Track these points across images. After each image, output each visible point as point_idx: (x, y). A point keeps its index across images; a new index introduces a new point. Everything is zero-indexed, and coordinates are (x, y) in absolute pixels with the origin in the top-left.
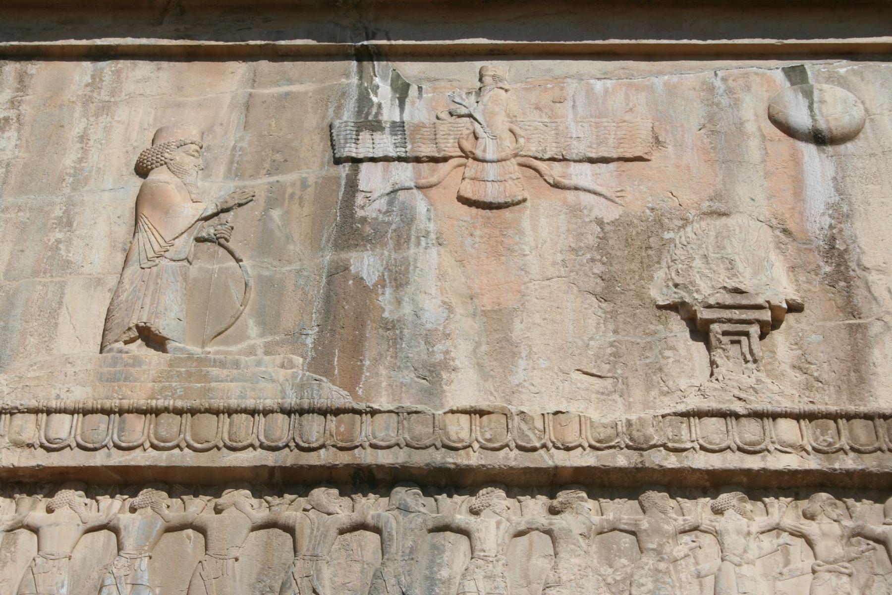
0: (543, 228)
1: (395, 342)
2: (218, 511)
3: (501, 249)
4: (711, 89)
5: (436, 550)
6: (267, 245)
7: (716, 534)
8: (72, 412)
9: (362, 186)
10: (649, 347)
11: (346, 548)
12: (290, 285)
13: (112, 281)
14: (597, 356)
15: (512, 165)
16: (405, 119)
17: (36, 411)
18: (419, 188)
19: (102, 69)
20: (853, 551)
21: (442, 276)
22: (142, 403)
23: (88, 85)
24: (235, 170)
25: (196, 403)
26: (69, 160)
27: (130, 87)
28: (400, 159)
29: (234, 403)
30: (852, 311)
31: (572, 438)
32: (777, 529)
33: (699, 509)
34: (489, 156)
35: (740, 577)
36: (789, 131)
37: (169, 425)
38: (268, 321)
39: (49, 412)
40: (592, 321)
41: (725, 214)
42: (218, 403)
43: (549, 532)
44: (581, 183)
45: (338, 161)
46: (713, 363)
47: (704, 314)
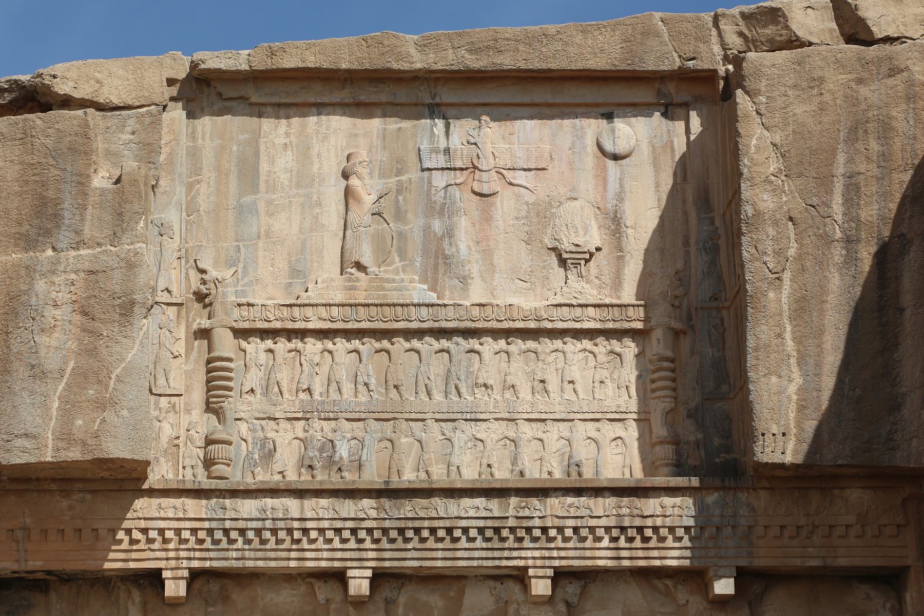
0: (506, 206)
2: (393, 344)
3: (487, 217)
7: (564, 353)
8: (338, 305)
10: (544, 268)
15: (493, 173)
16: (450, 146)
18: (456, 185)
21: (466, 233)
22: (363, 301)
24: (382, 175)
25: (382, 301)
28: (448, 169)
29: (395, 301)
31: (515, 316)
33: (558, 344)
34: (484, 168)
35: (570, 370)
38: (402, 254)
42: (389, 301)
43: (507, 353)
45: (423, 170)
46: (566, 276)
47: (565, 256)
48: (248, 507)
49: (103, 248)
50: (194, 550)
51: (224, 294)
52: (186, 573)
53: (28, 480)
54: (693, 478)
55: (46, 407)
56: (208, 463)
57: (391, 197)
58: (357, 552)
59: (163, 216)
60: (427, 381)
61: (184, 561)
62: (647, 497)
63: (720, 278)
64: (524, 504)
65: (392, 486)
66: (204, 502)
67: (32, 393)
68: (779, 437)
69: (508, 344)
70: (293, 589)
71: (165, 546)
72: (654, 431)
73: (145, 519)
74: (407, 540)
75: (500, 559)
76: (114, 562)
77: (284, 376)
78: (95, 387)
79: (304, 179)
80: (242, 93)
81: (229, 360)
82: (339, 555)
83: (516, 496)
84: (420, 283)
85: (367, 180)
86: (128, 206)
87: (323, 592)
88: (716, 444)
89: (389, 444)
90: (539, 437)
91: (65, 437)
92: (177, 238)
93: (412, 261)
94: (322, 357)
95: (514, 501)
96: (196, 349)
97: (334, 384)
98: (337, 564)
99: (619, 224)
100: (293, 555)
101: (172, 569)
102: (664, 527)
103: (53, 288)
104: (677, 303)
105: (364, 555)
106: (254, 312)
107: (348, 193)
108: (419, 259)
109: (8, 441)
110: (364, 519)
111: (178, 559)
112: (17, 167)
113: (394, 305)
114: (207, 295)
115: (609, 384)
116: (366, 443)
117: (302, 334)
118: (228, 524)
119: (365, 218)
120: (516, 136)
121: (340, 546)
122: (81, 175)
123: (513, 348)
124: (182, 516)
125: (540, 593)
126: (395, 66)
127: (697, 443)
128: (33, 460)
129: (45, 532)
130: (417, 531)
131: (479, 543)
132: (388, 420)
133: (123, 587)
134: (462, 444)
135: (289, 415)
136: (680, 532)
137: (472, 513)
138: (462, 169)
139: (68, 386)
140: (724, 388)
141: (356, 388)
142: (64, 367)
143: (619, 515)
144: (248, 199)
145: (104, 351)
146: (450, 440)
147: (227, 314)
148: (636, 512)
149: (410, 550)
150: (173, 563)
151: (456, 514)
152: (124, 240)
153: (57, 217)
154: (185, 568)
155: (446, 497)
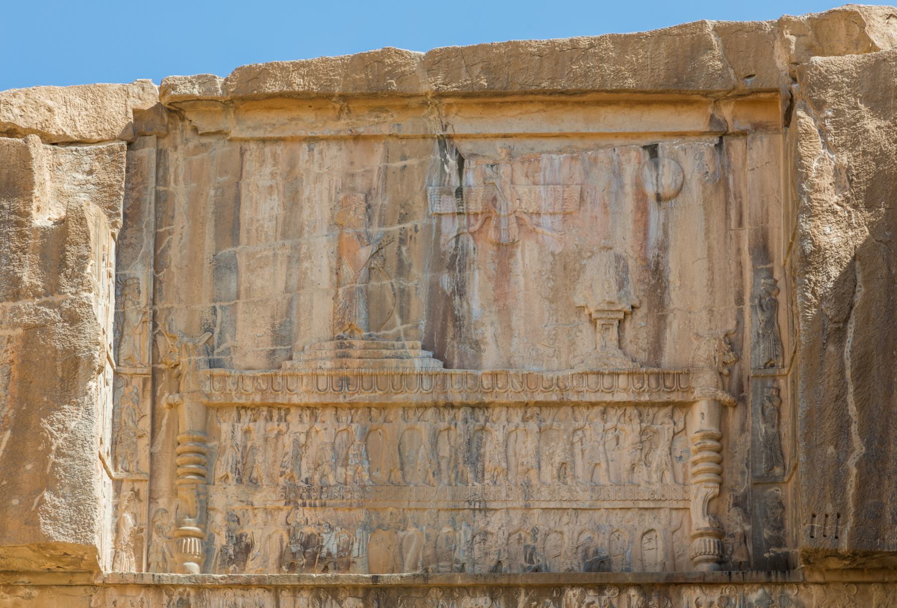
0: (527, 260)
9: (444, 230)
12: (413, 292)
13: (333, 292)
14: (549, 335)
19: (313, 150)
20: (644, 438)
23: (307, 162)
27: (328, 162)
28: (459, 214)
38: (405, 316)
40: (547, 315)
41: (611, 248)
47: (594, 316)
59: (127, 272)
63: (778, 341)
72: (694, 521)
79: (290, 229)
80: (222, 127)
84: (424, 348)
88: (766, 536)
90: (559, 529)
92: (143, 300)
96: (164, 428)
104: (726, 371)
119: (363, 271)
120: (542, 174)
127: (744, 536)
134: (469, 537)
140: (778, 470)
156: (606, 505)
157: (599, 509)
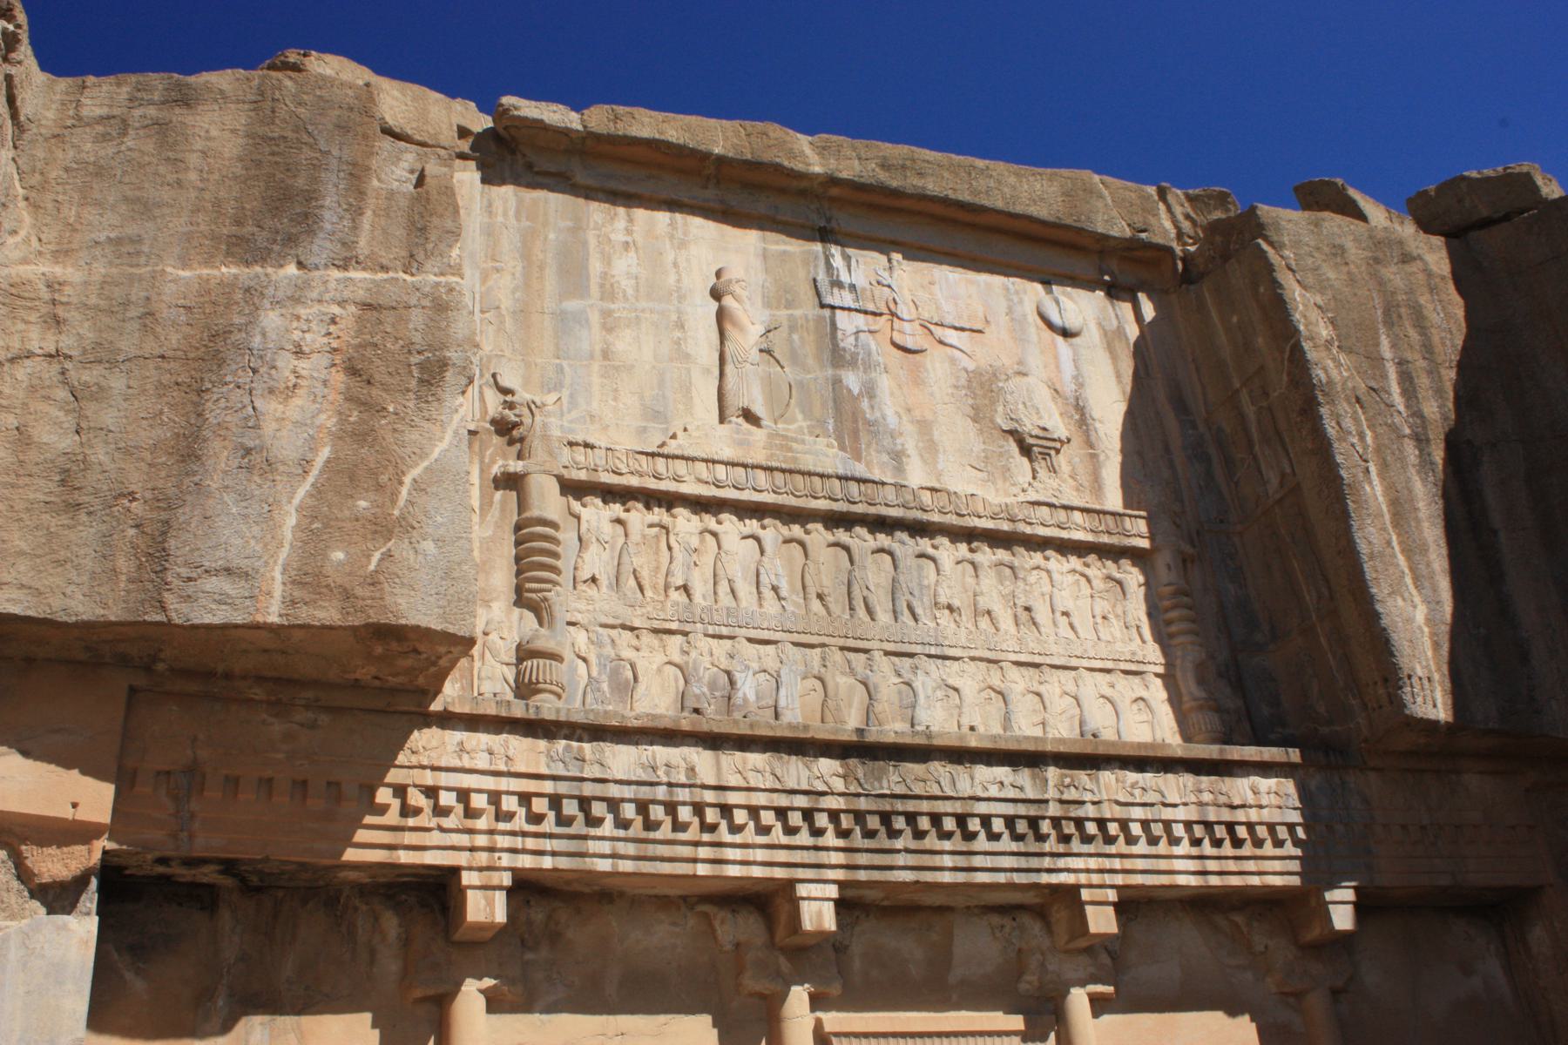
1: (876, 434)
2: (807, 532)
3: (917, 380)
4: (1007, 289)
5: (920, 568)
6: (795, 358)
7: (1048, 572)
8: (726, 464)
9: (839, 325)
10: (1001, 455)
11: (875, 562)
17: (706, 461)
21: (892, 394)
22: (764, 463)
24: (767, 304)
25: (792, 466)
26: (672, 279)
28: (856, 310)
29: (811, 468)
30: (1092, 446)
31: (981, 511)
32: (1074, 571)
33: (1037, 558)
34: (906, 317)
36: (1050, 325)
37: (779, 476)
38: (807, 414)
39: (714, 462)
41: (1025, 375)
42: (802, 467)
43: (972, 563)
44: (954, 343)
45: (822, 306)
46: (1034, 470)
47: (1031, 441)
48: (623, 760)
49: (391, 274)
50: (524, 834)
51: (545, 425)
52: (507, 879)
53: (210, 675)
54: (1290, 750)
55: (269, 519)
56: (525, 689)
57: (783, 332)
58: (812, 852)
60: (866, 592)
61: (505, 856)
62: (1231, 775)
64: (1067, 780)
65: (872, 737)
66: (542, 744)
67: (244, 497)
68: (1425, 682)
69: (972, 550)
70: (674, 924)
71: (469, 823)
73: (434, 769)
74: (894, 834)
75: (1038, 871)
76: (367, 848)
77: (640, 560)
78: (372, 496)
81: (554, 525)
82: (782, 856)
83: (1057, 766)
85: (747, 305)
86: (435, 221)
87: (734, 929)
89: (818, 684)
91: (307, 579)
93: (822, 423)
94: (702, 541)
95: (1052, 773)
97: (723, 588)
98: (779, 873)
99: (1083, 415)
100: (703, 852)
101: (480, 869)
102: (1261, 824)
103: (295, 324)
105: (825, 857)
106: (597, 458)
107: (721, 316)
108: (831, 421)
109: (190, 579)
110: (823, 794)
111: (491, 849)
112: (240, 141)
113: (810, 474)
114: (516, 425)
115: (1114, 620)
116: (784, 679)
117: (669, 501)
118: (588, 789)
120: (937, 287)
121: (785, 840)
122: (355, 165)
123: (978, 557)
124: (503, 768)
125: (1102, 930)
126: (786, 163)
128: (239, 619)
129: (233, 783)
130: (911, 818)
131: (1006, 844)
132: (812, 646)
133: (364, 908)
134: (930, 692)
135: (657, 624)
136: (1282, 833)
137: (994, 791)
138: (874, 314)
139: (318, 491)
141: (759, 593)
142: (309, 456)
143: (1201, 804)
144: (572, 305)
145: (390, 438)
146: (908, 684)
147: (551, 454)
148: (1222, 799)
149: (898, 851)
150: (483, 858)
151: (968, 792)
152: (428, 266)
153: (307, 221)
154: (505, 869)
155: (952, 762)
156: (1086, 663)
157: (1075, 669)
